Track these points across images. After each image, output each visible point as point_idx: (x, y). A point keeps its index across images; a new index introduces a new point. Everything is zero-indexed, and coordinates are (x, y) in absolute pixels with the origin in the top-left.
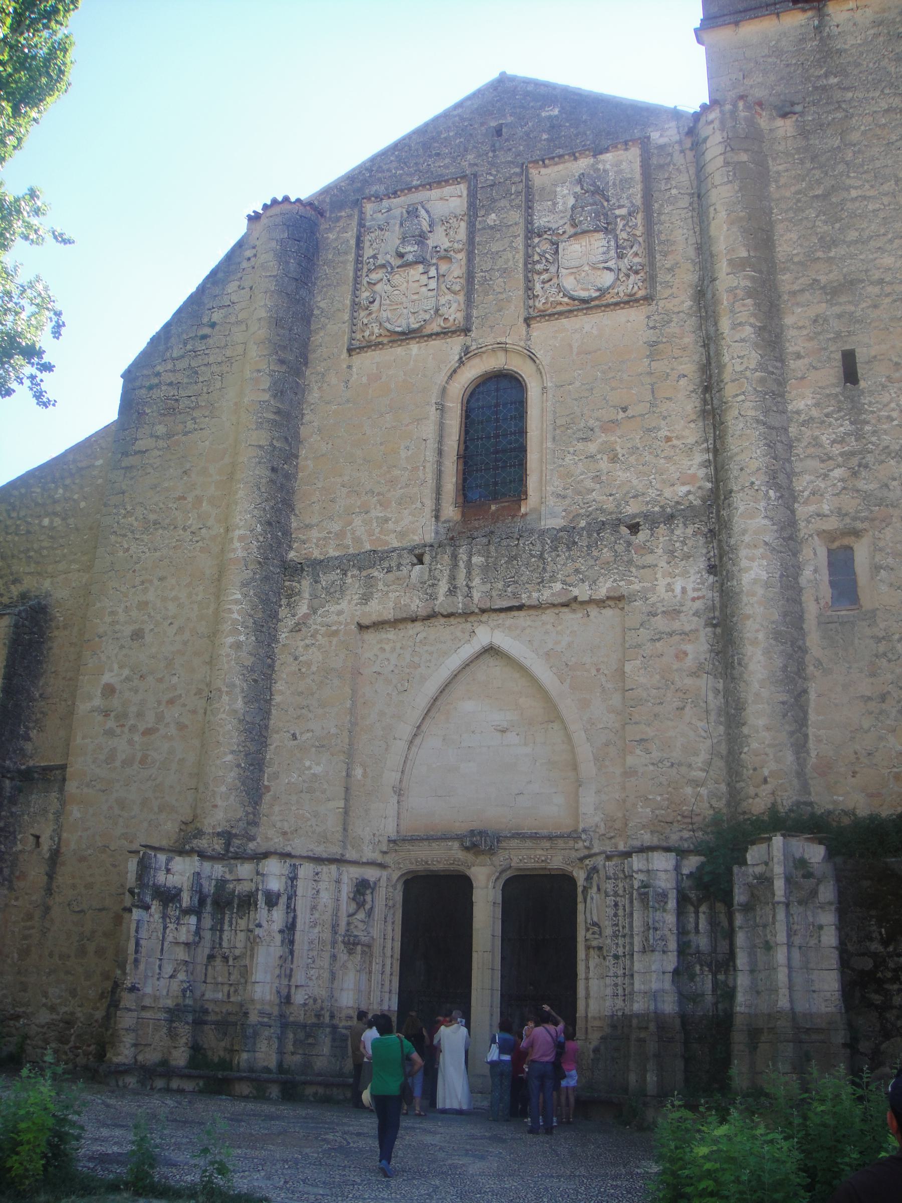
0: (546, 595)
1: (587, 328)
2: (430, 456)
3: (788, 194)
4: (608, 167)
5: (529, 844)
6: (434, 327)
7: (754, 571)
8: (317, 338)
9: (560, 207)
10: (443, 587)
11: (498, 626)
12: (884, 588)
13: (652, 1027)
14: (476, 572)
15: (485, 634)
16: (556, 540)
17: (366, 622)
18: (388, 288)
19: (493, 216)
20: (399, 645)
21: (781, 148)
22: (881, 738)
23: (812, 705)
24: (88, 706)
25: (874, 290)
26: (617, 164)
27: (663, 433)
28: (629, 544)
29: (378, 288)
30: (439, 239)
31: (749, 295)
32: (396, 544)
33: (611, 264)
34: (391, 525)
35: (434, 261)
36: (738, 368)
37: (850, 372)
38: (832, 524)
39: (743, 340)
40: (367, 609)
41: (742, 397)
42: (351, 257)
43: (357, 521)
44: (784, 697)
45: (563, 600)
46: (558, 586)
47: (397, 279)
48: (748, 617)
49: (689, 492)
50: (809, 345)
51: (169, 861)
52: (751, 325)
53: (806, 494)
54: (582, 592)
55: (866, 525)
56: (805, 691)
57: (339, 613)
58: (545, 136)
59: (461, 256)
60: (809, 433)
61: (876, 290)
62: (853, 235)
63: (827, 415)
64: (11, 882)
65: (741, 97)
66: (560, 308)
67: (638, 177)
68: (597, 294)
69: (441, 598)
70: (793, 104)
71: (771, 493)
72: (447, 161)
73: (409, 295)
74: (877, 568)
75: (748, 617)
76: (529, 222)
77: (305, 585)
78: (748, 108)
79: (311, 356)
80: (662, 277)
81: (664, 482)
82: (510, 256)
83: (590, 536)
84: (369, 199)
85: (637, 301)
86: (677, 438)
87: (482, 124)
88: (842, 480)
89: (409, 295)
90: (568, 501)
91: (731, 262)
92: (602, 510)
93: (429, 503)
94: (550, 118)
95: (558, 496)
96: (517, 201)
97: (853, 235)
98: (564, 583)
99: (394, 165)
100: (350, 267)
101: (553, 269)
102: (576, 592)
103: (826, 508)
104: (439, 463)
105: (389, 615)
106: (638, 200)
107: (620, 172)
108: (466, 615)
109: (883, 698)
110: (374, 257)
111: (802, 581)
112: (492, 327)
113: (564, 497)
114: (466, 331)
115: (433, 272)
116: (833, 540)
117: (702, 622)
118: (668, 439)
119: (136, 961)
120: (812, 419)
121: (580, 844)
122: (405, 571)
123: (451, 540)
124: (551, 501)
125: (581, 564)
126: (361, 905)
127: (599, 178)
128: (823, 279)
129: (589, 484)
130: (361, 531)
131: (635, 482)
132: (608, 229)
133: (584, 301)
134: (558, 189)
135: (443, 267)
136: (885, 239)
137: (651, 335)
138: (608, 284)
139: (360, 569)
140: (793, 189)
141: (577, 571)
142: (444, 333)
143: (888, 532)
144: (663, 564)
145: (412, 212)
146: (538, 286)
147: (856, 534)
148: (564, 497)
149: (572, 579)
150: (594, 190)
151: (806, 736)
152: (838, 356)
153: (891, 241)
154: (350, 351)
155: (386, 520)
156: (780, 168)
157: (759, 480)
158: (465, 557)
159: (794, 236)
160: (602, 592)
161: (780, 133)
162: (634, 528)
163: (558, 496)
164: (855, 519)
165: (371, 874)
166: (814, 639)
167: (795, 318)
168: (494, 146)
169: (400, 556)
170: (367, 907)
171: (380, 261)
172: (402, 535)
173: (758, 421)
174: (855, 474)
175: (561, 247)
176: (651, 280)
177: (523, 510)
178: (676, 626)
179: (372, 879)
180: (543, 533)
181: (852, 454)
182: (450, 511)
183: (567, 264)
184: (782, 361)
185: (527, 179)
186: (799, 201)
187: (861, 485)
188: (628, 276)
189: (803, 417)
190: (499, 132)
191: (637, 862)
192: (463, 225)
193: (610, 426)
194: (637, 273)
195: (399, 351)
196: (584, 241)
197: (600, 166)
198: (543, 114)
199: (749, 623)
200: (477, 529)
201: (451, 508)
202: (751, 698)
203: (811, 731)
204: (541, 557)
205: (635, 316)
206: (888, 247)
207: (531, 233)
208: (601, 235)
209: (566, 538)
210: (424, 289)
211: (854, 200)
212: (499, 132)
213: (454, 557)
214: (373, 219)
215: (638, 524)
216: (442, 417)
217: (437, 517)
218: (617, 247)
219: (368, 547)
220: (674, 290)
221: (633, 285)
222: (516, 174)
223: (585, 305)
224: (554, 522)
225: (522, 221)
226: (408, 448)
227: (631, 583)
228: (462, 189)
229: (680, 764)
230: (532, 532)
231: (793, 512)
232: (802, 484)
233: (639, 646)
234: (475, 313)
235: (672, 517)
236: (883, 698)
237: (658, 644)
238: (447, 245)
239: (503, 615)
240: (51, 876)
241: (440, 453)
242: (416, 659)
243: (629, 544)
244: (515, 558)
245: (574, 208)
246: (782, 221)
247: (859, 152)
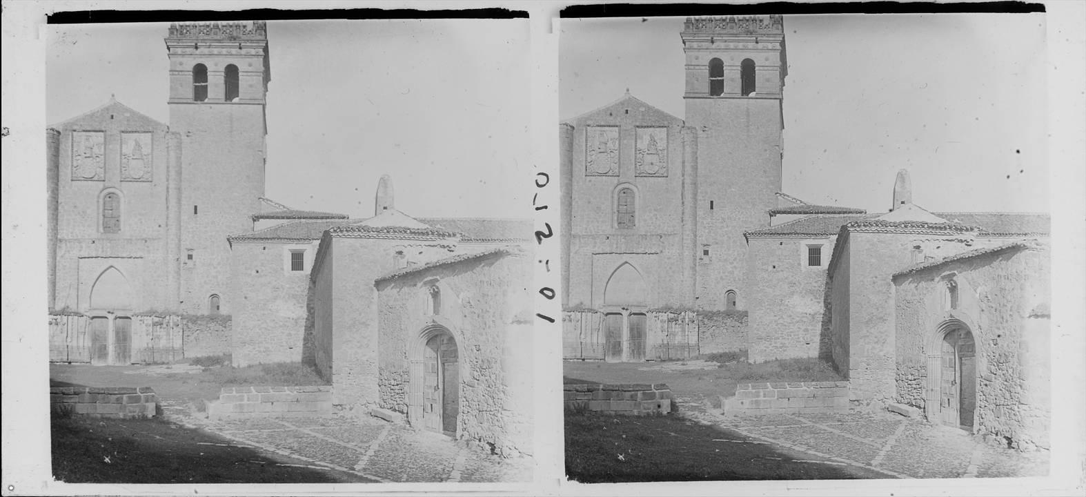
15: (625, 258)
34: (600, 228)
77: (577, 241)
102: (647, 251)
150: (653, 141)
160: (653, 252)
172: (603, 231)
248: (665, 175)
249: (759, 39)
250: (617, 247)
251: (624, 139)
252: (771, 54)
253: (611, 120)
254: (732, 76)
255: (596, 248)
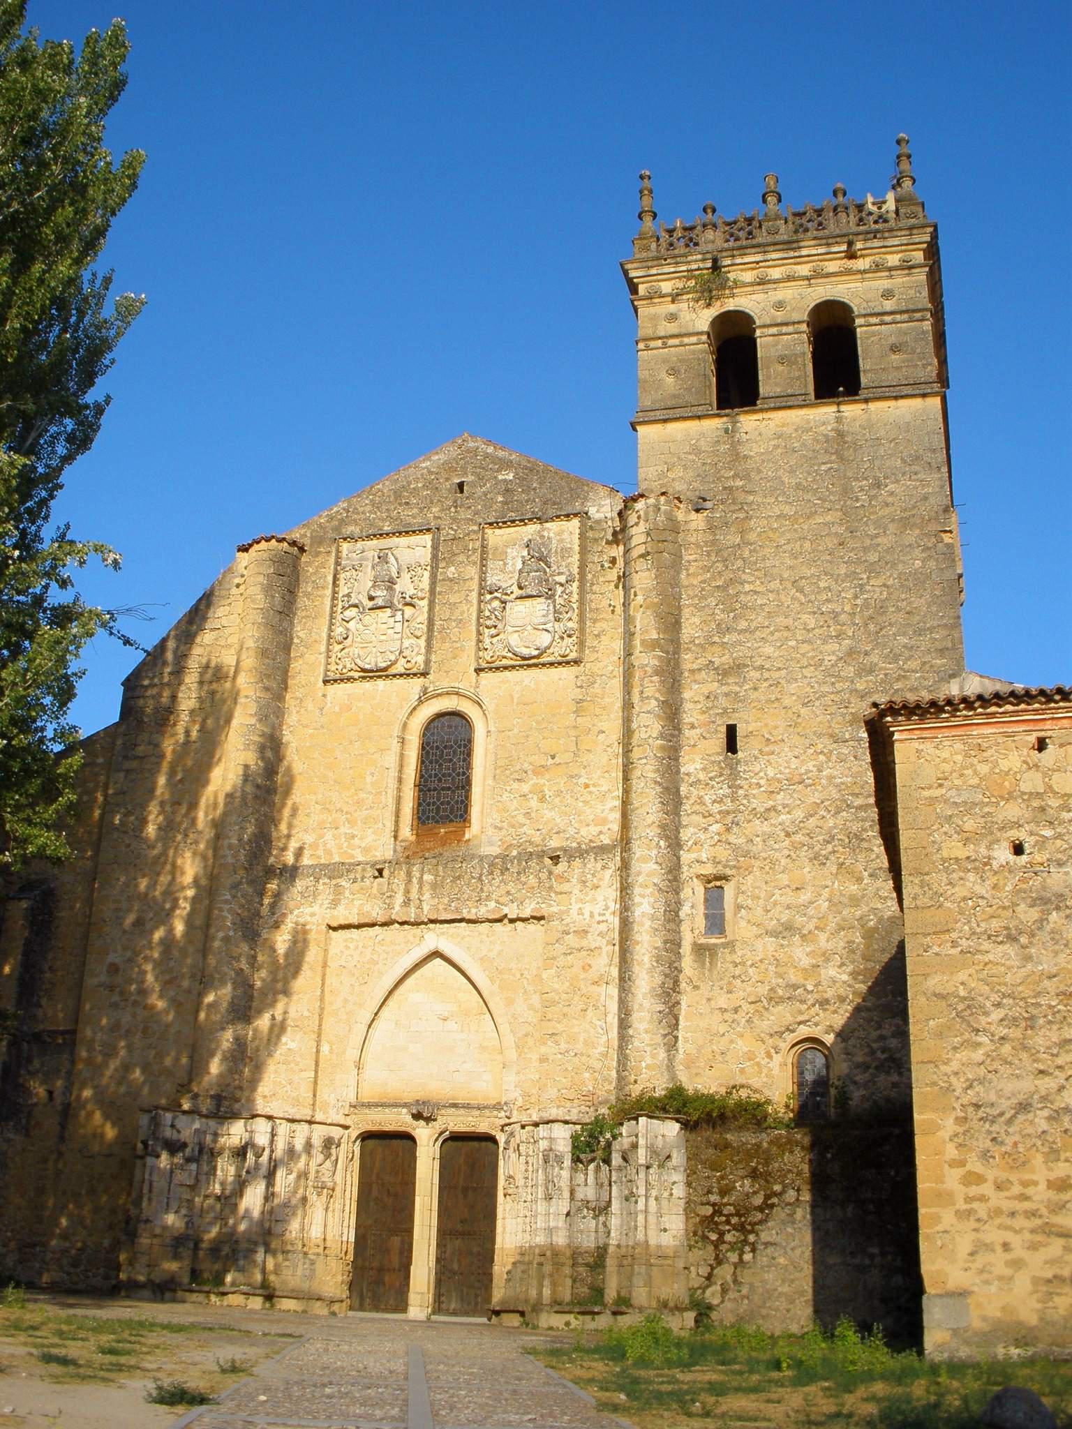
0: (482, 912)
1: (526, 682)
2: (393, 784)
3: (695, 582)
4: (552, 535)
5: (462, 1111)
6: (399, 668)
7: (646, 906)
8: (295, 666)
9: (509, 568)
10: (399, 898)
11: (443, 934)
12: (743, 924)
13: (548, 1253)
14: (426, 888)
15: (433, 939)
16: (492, 865)
17: (335, 924)
18: (360, 626)
19: (452, 569)
20: (361, 945)
21: (693, 540)
22: (732, 1041)
23: (683, 1012)
24: (95, 981)
25: (755, 675)
26: (559, 533)
27: (582, 780)
28: (550, 873)
29: (351, 625)
30: (405, 585)
31: (657, 673)
32: (361, 858)
33: (549, 626)
35: (400, 607)
36: (643, 736)
37: (732, 746)
38: (709, 870)
39: (649, 712)
40: (336, 912)
41: (644, 761)
42: (329, 592)
43: (329, 836)
44: (661, 1007)
45: (497, 916)
46: (492, 905)
47: (367, 619)
48: (638, 943)
49: (601, 833)
50: (702, 717)
51: (174, 1118)
52: (656, 699)
53: (690, 843)
54: (512, 912)
55: (733, 872)
56: (678, 1003)
57: (313, 915)
58: (500, 499)
59: (425, 603)
60: (696, 792)
61: (757, 675)
62: (743, 624)
63: (711, 779)
64: (27, 1130)
65: (663, 494)
66: (505, 662)
67: (577, 548)
68: (536, 653)
69: (397, 908)
70: (705, 500)
71: (662, 843)
72: (415, 511)
73: (377, 637)
74: (739, 907)
75: (638, 943)
76: (482, 580)
78: (668, 502)
79: (290, 682)
80: (590, 642)
81: (581, 822)
82: (465, 608)
83: (519, 863)
84: (345, 539)
85: (568, 663)
86: (594, 785)
87: (447, 479)
88: (719, 834)
89: (377, 637)
90: (504, 832)
91: (643, 642)
92: (531, 843)
93: (390, 825)
94: (505, 480)
95: (496, 827)
96: (473, 558)
97: (743, 624)
98: (497, 902)
99: (369, 508)
100: (328, 602)
101: (500, 626)
102: (506, 910)
103: (704, 857)
104: (399, 790)
105: (354, 920)
106: (576, 571)
107: (561, 541)
108: (416, 924)
109: (736, 1010)
110: (348, 595)
111: (682, 914)
112: (447, 672)
113: (500, 829)
114: (424, 674)
115: (399, 616)
116: (709, 882)
117: (604, 941)
118: (587, 786)
119: (150, 1199)
120: (699, 780)
121: (503, 1114)
122: (368, 882)
123: (408, 857)
124: (490, 831)
125: (511, 887)
126: (328, 1156)
127: (543, 544)
128: (717, 661)
129: (521, 819)
130: (331, 844)
131: (558, 820)
132: (550, 597)
133: (524, 659)
134: (509, 551)
135: (409, 611)
136: (768, 631)
137: (578, 693)
138: (546, 644)
139: (330, 878)
140: (700, 578)
141: (508, 893)
142: (406, 675)
143: (750, 878)
144: (576, 891)
145: (383, 559)
146: (487, 641)
147: (725, 878)
148: (500, 829)
149: (505, 899)
150: (539, 556)
151: (676, 1038)
152: (724, 729)
153: (772, 633)
154: (325, 682)
155: (353, 837)
156: (691, 558)
157: (653, 832)
158: (418, 875)
159: (697, 620)
160: (527, 913)
161: (693, 526)
162: (555, 859)
163: (496, 827)
164: (725, 866)
165: (336, 1132)
166: (688, 963)
167: (692, 693)
168: (455, 501)
169: (364, 870)
170: (333, 1158)
171: (354, 601)
172: (366, 850)
173: (656, 782)
174: (728, 830)
175: (509, 605)
176: (581, 644)
177: (467, 836)
178: (584, 943)
179: (337, 1137)
180: (481, 859)
181: (728, 813)
182: (406, 832)
183: (513, 623)
184: (680, 730)
185: (483, 539)
186: (703, 589)
187: (732, 839)
188: (562, 638)
189: (692, 779)
190: (461, 486)
191: (542, 1131)
192: (427, 574)
193: (540, 770)
194: (570, 636)
195: (367, 685)
196: (528, 602)
197: (545, 534)
198: (500, 477)
199: (637, 947)
200: (429, 850)
201: (408, 829)
202: (636, 1007)
203: (681, 1034)
204: (480, 879)
205: (567, 673)
206: (770, 638)
207: (484, 589)
208: (542, 600)
209: (500, 864)
210: (391, 631)
211: (746, 593)
212: (461, 486)
213: (409, 874)
214: (348, 559)
215: (558, 857)
216: (403, 749)
217: (396, 837)
218: (555, 612)
219: (337, 859)
220: (600, 654)
221: (567, 647)
222: (474, 532)
223: (528, 662)
224: (491, 850)
225: (477, 577)
226: (372, 774)
227: (551, 906)
228: (427, 538)
229: (582, 1054)
230: (473, 857)
231: (679, 858)
232: (685, 835)
233: (554, 958)
234: (433, 657)
235: (587, 852)
236: (736, 1010)
237: (569, 958)
238: (412, 592)
239: (446, 925)
240: (63, 1127)
241: (400, 780)
242: (375, 957)
243: (550, 873)
244: (459, 878)
245: (521, 572)
246: (689, 606)
247: (755, 550)
248: (573, 655)
249: (859, 245)
250: (407, 903)
251: (450, 562)
252: (900, 280)
253: (410, 515)
254: (783, 354)
255: (341, 908)
